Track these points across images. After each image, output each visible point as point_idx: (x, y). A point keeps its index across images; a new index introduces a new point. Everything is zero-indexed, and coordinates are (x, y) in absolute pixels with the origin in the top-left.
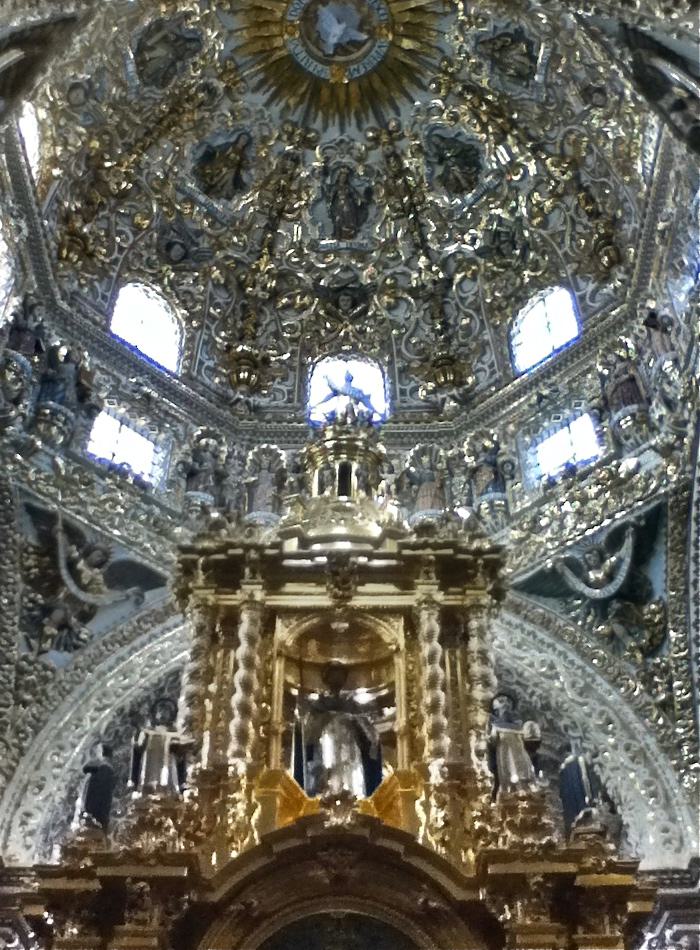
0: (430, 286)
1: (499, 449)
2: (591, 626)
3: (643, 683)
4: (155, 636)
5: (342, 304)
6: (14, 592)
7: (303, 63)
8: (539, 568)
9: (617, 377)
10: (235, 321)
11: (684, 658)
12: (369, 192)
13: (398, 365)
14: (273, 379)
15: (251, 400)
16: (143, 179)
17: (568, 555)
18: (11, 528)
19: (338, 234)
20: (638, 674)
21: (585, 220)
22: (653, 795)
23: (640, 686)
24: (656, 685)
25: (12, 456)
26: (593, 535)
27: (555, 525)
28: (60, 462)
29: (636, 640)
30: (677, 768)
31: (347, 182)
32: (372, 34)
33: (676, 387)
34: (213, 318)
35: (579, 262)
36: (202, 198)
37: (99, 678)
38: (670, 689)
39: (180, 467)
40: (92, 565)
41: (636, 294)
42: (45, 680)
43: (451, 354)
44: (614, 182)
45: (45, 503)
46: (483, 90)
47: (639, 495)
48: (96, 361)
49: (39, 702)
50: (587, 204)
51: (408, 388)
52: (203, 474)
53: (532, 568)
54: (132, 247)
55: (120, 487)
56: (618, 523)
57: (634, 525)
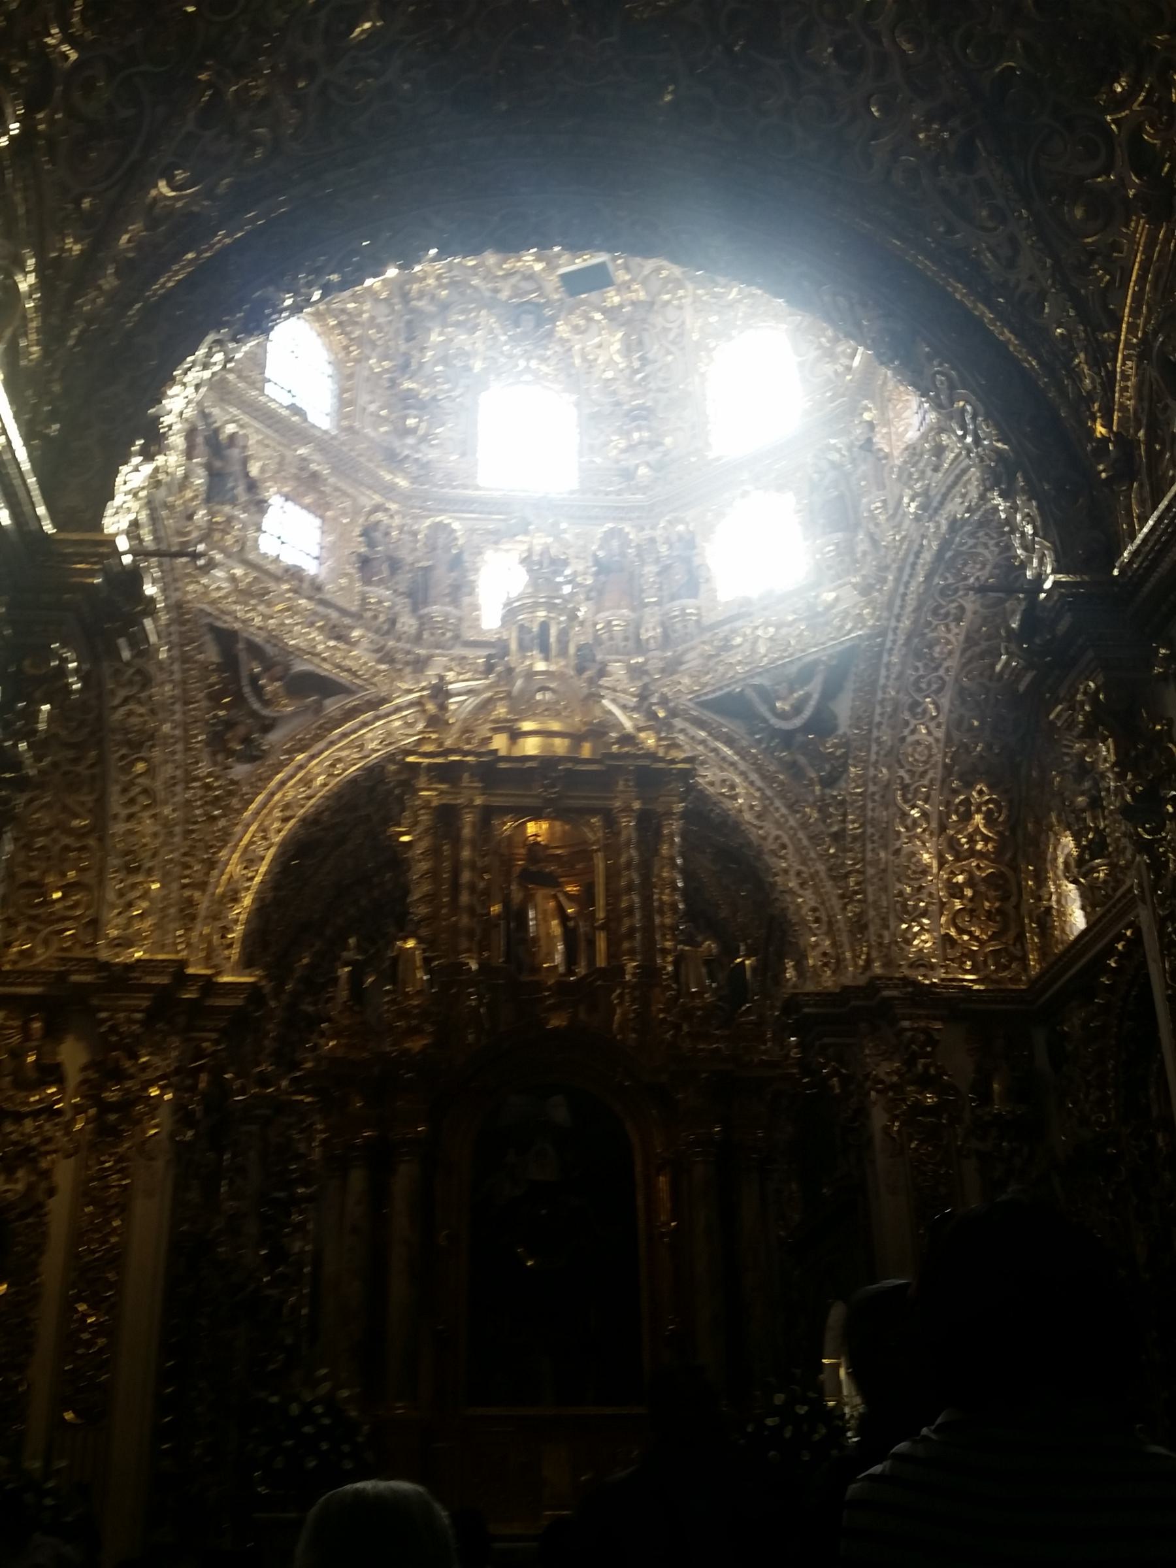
3: (820, 811)
8: (726, 690)
11: (860, 794)
17: (757, 681)
22: (817, 920)
23: (816, 815)
24: (830, 816)
29: (818, 771)
38: (844, 821)
39: (354, 558)
42: (231, 794)
53: (721, 688)
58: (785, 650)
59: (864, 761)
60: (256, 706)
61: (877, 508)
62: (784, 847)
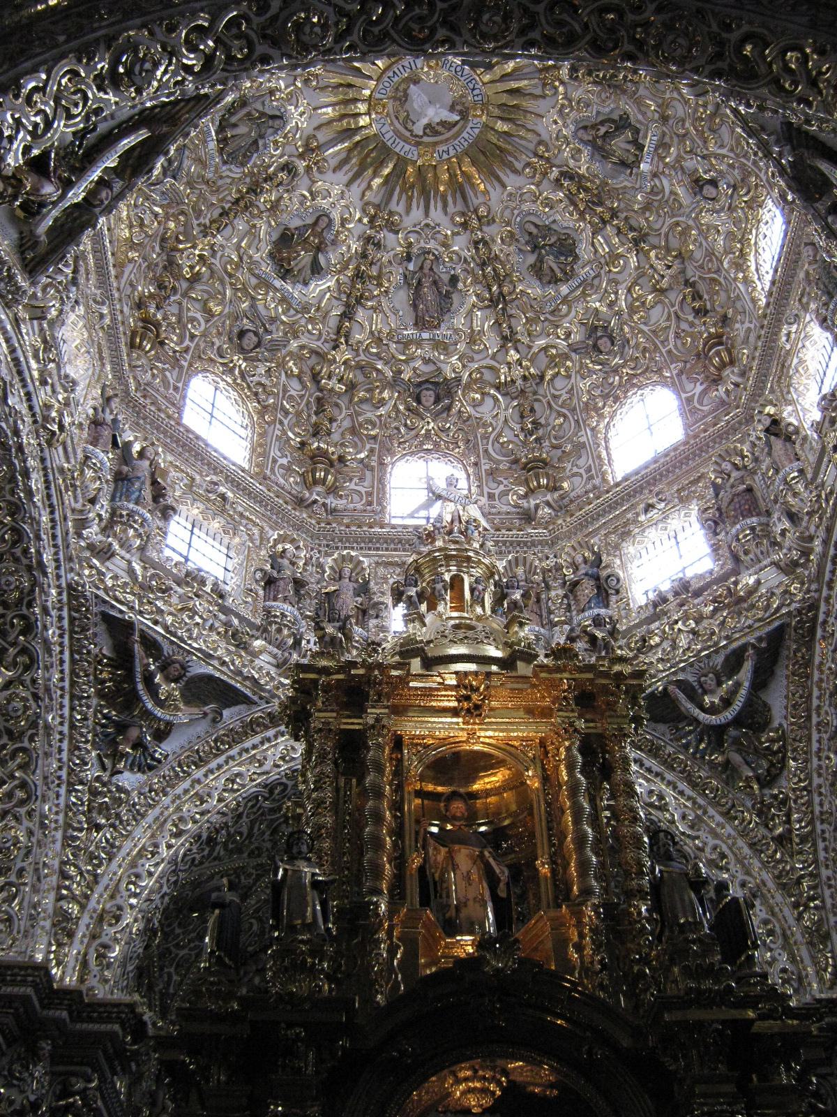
0: (519, 382)
1: (601, 561)
2: (704, 753)
3: (758, 815)
4: (232, 758)
5: (423, 399)
6: (89, 707)
7: (389, 144)
9: (732, 486)
10: (309, 416)
11: (805, 788)
12: (454, 280)
13: (485, 466)
14: (351, 480)
15: (328, 501)
16: (217, 262)
17: (681, 677)
18: (87, 639)
19: (420, 323)
20: (753, 806)
21: (691, 318)
22: (771, 933)
25: (88, 560)
26: (708, 656)
27: (666, 645)
28: (137, 567)
29: (753, 769)
30: (796, 905)
31: (431, 269)
32: (464, 115)
33: (802, 500)
34: (287, 413)
35: (686, 362)
36: (278, 283)
37: (173, 802)
38: (788, 821)
39: (259, 575)
40: (168, 679)
41: (754, 397)
42: (119, 802)
43: (544, 455)
44: (725, 278)
45: (121, 612)
46: (581, 177)
47: (760, 614)
48: (170, 458)
49: (113, 826)
50: (694, 299)
51: (497, 492)
52: (281, 583)
54: (204, 335)
55: (198, 596)
56: (735, 645)
57: (753, 646)
58: (710, 639)
59: (806, 753)
60: (150, 705)
61: (794, 478)
62: (723, 856)
